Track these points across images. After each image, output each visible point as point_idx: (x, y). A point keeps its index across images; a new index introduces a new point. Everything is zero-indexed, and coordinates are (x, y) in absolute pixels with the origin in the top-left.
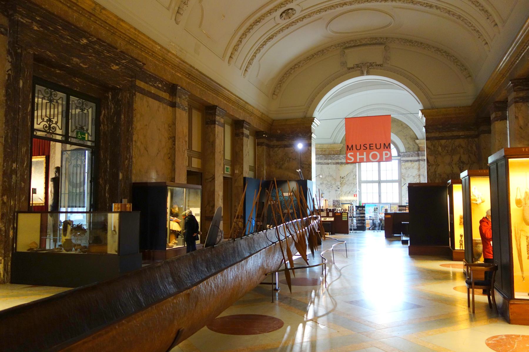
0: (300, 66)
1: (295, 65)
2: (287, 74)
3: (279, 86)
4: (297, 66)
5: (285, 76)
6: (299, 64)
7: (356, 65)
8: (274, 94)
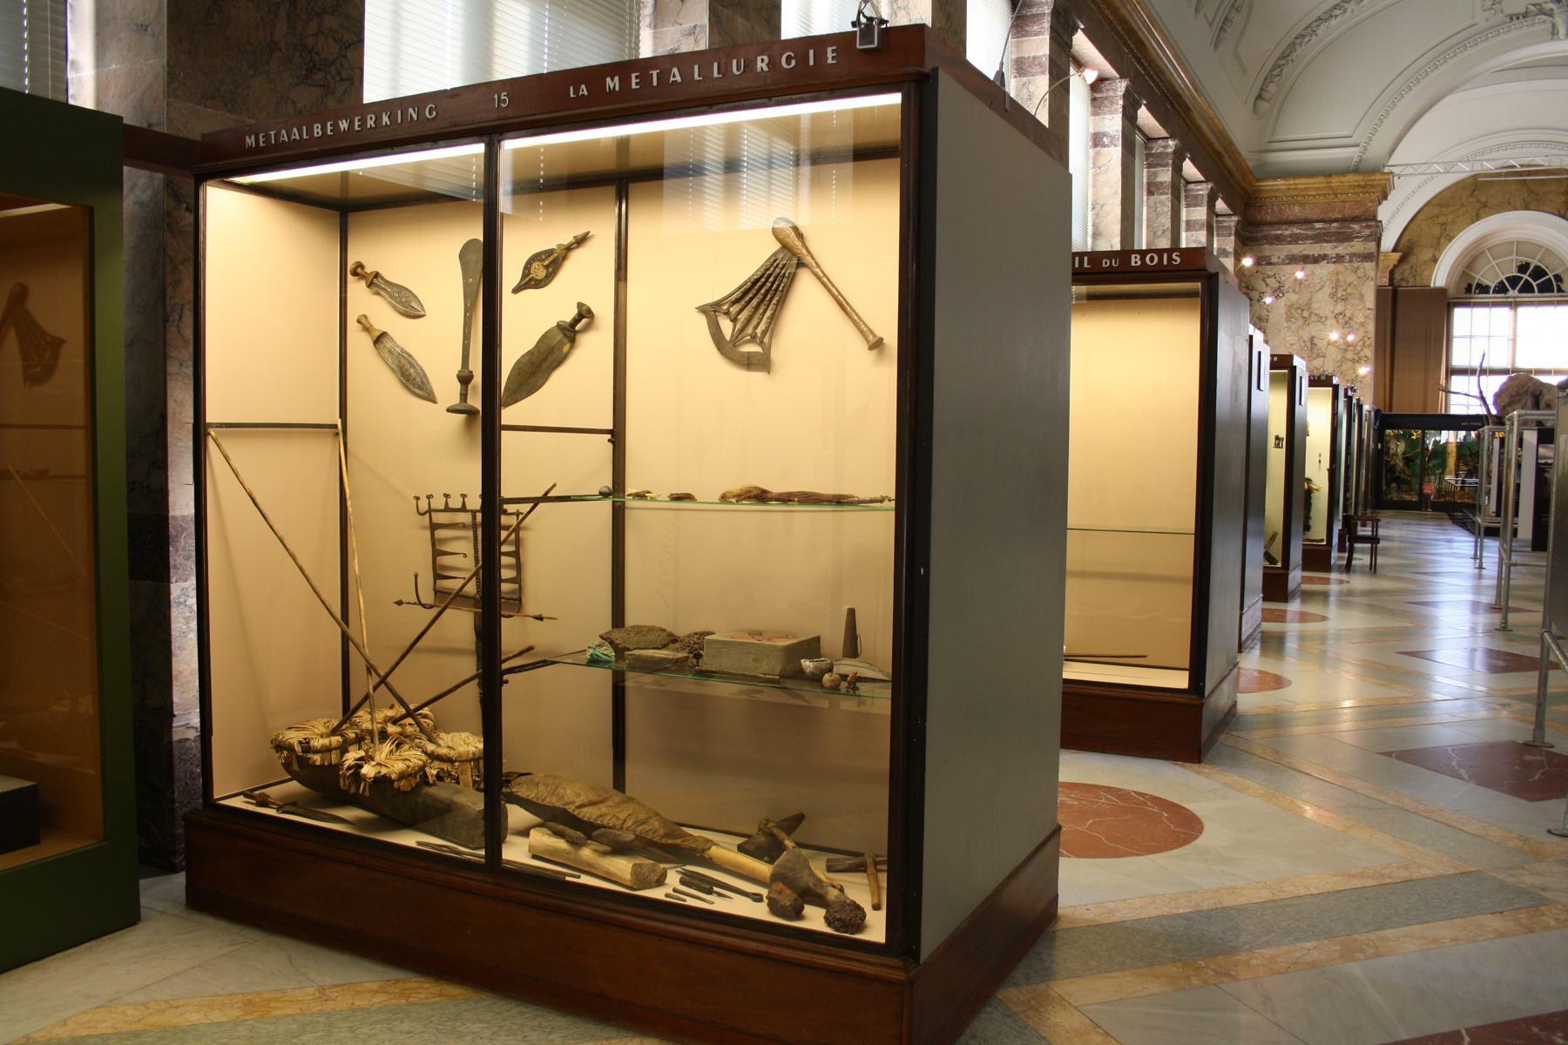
0: (1349, 11)
1: (1334, 8)
2: (1303, 36)
3: (1275, 73)
4: (1337, 12)
5: (1299, 41)
6: (1346, 5)
7: (1534, 5)
8: (1259, 97)
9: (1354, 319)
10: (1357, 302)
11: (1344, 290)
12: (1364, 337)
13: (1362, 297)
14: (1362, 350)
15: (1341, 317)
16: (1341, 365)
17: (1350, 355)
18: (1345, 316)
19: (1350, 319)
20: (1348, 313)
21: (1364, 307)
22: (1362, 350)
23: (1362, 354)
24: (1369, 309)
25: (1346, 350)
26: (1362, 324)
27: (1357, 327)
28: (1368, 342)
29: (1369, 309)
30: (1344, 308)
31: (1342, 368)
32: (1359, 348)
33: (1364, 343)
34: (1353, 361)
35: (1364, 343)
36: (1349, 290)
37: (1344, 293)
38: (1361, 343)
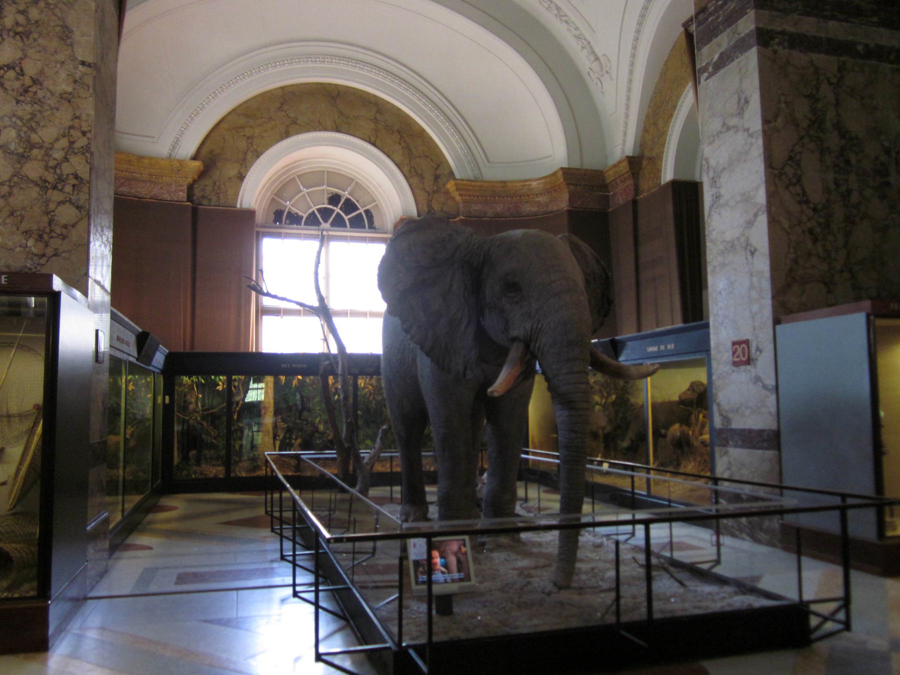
9: (46, 84)
10: (55, 43)
11: (22, 12)
12: (71, 127)
13: (65, 35)
14: (66, 159)
15: (11, 74)
16: (10, 194)
17: (33, 170)
18: (22, 73)
19: (35, 81)
20: (31, 69)
21: (73, 58)
22: (66, 159)
23: (66, 169)
24: (83, 63)
25: (22, 158)
26: (67, 98)
27: (52, 102)
28: (81, 142)
29: (83, 63)
30: (19, 54)
31: (11, 200)
32: (58, 155)
33: (72, 143)
34: (43, 185)
35: (72, 143)
36: (34, 13)
37: (21, 19)
38: (64, 143)
